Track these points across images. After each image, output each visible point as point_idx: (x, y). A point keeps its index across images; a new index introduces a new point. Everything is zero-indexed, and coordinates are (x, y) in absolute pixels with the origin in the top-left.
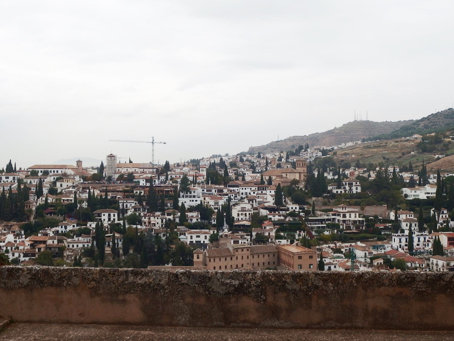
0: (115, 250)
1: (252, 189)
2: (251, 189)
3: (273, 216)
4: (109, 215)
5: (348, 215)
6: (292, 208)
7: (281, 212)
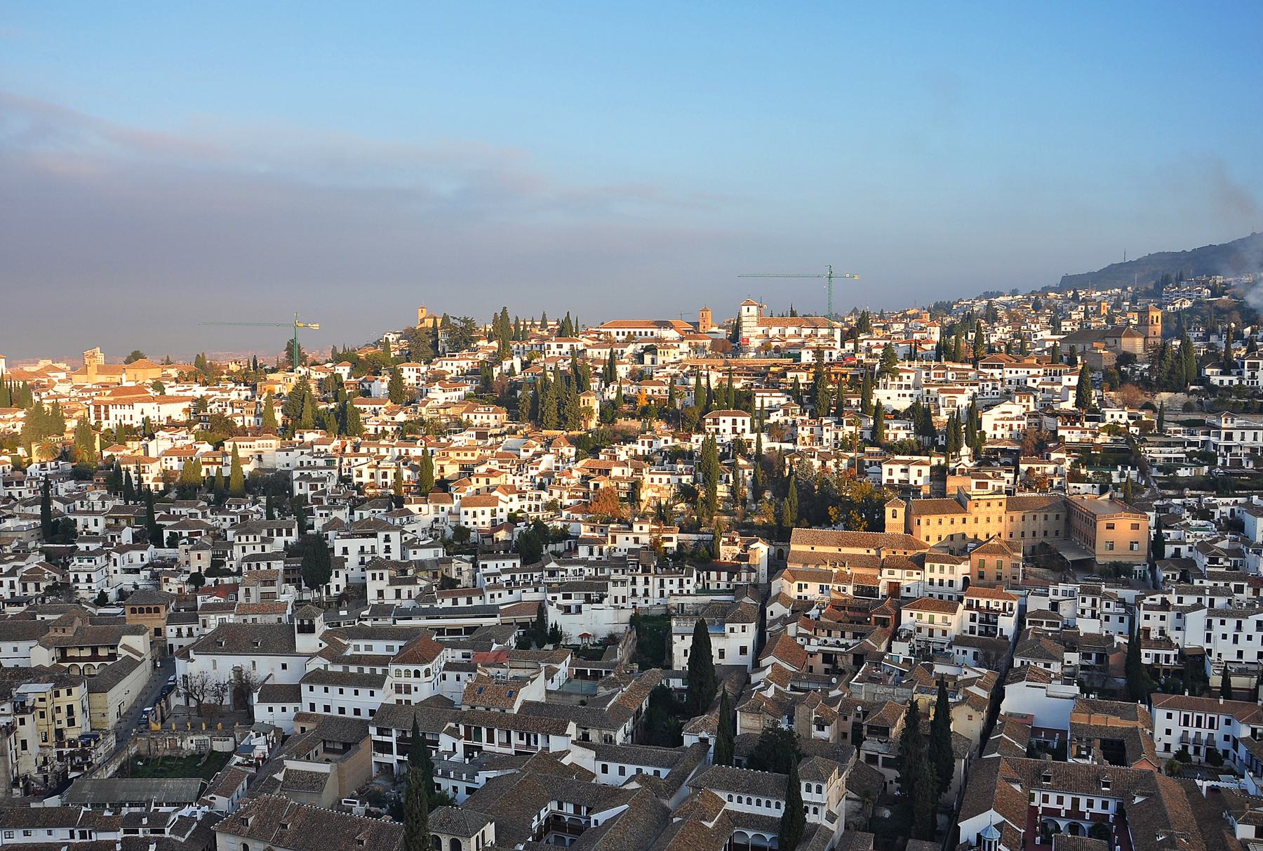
1: (1031, 373)
2: (1028, 372)
4: (734, 422)
5: (1237, 435)
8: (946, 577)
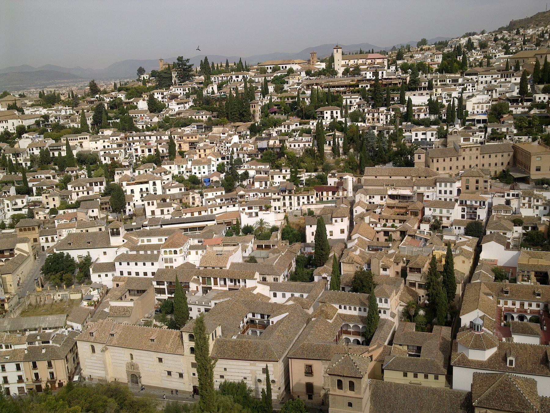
0: (335, 150)
1: (494, 77)
2: (492, 77)
3: (515, 109)
4: (332, 113)
6: (540, 98)
7: (525, 104)
8: (448, 189)
